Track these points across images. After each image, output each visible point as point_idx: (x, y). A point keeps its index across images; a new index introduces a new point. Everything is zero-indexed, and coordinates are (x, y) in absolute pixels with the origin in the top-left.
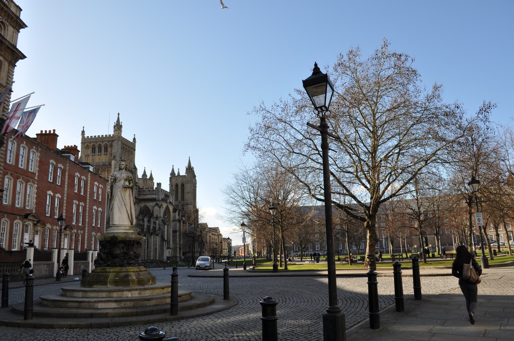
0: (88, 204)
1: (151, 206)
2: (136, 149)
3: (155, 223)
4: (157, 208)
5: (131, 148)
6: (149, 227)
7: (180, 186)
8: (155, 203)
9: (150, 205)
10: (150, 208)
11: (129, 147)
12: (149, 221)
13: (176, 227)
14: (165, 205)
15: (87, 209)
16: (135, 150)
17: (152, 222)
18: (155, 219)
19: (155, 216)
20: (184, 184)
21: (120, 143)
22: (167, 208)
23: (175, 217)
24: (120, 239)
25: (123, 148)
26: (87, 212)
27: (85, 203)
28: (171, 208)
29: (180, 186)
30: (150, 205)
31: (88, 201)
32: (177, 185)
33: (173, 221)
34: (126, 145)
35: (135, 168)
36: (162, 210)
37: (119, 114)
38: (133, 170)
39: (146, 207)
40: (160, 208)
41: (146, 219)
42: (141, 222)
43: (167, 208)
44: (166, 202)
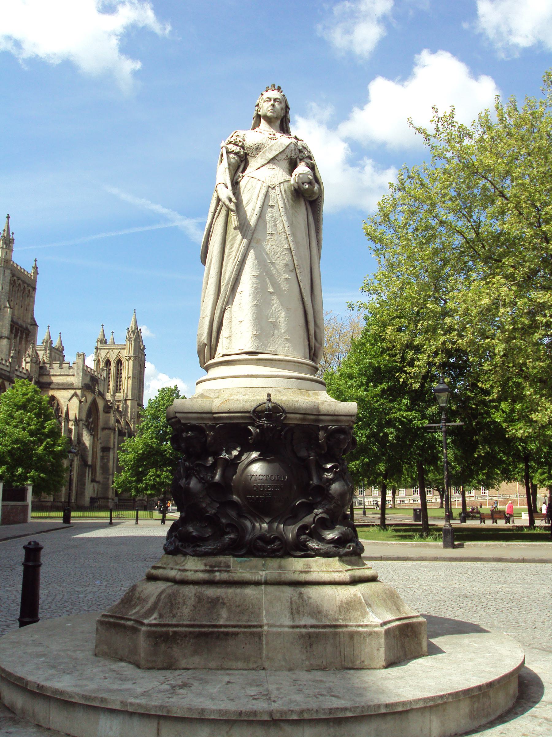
2: (38, 287)
5: (28, 285)
7: (113, 364)
8: (71, 392)
11: (24, 282)
13: (109, 441)
16: (34, 289)
20: (123, 360)
21: (8, 272)
22: (94, 403)
23: (107, 422)
24: (294, 420)
25: (13, 283)
29: (113, 364)
32: (108, 363)
33: (104, 429)
34: (19, 279)
35: (35, 325)
37: (8, 217)
38: (29, 326)
44: (93, 392)
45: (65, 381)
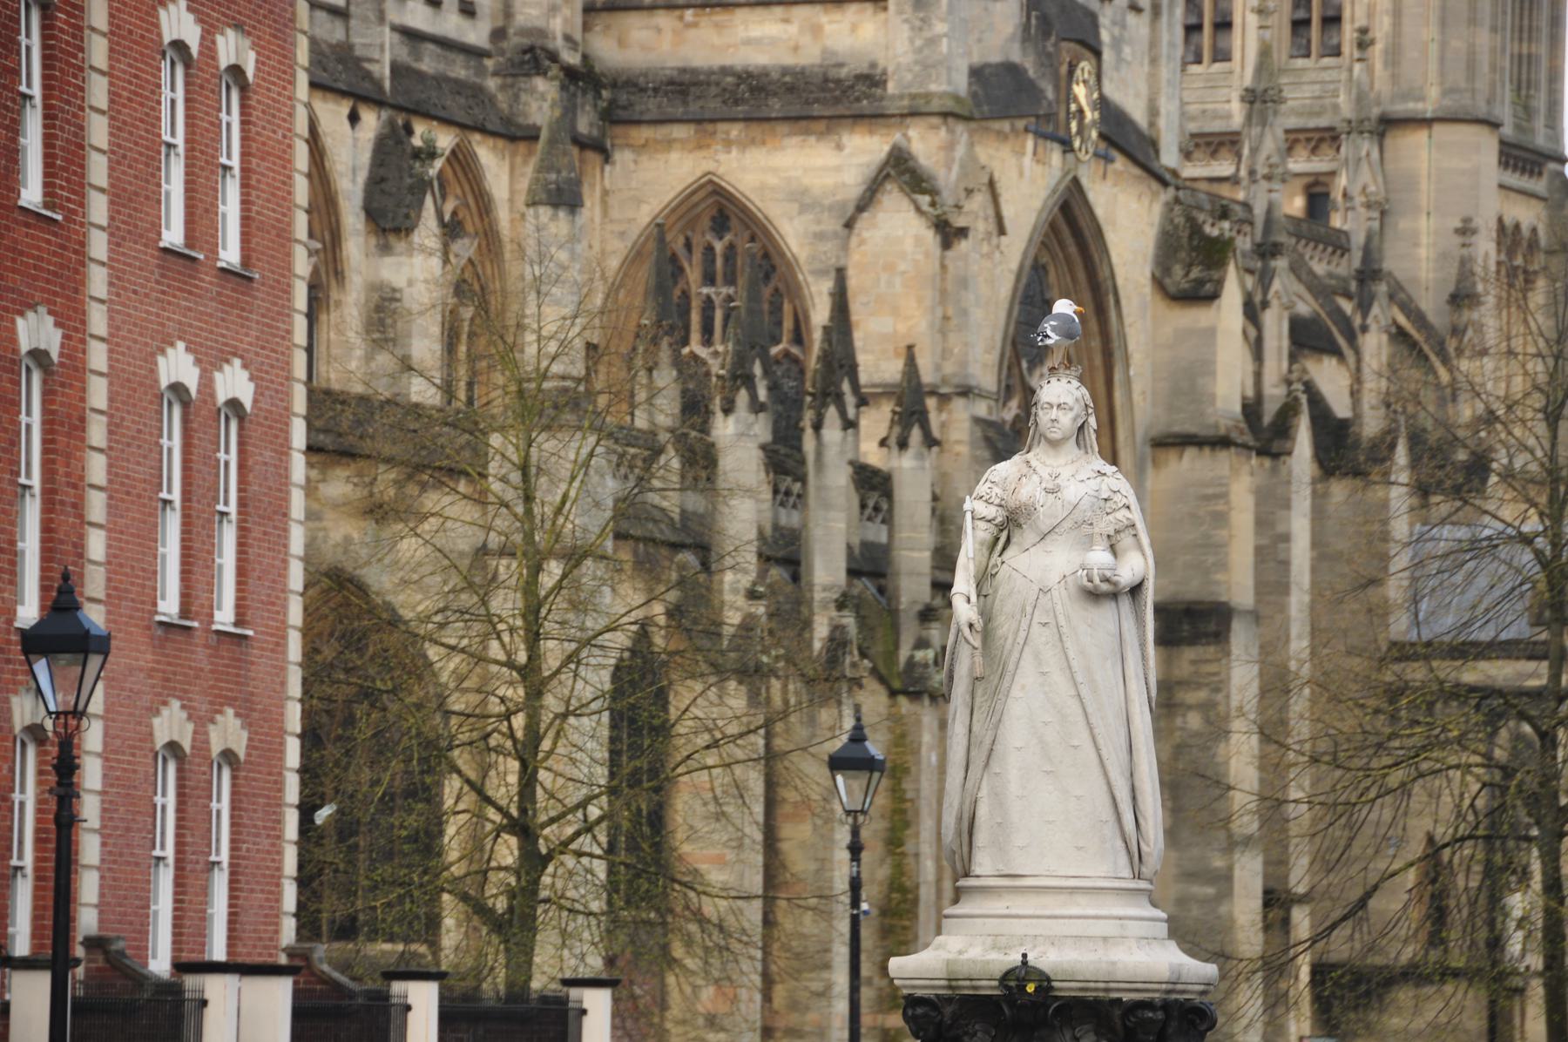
0: (98, 321)
1: (803, 201)
3: (873, 486)
4: (899, 226)
6: (784, 553)
8: (864, 150)
9: (792, 178)
10: (795, 235)
12: (785, 463)
14: (1026, 179)
15: (98, 394)
17: (839, 478)
18: (876, 421)
19: (877, 364)
22: (1071, 231)
26: (97, 432)
27: (72, 321)
28: (1130, 221)
30: (792, 178)
31: (98, 281)
36: (995, 268)
39: (719, 208)
40: (948, 233)
41: (739, 437)
42: (669, 495)
43: (1071, 231)
45: (809, 56)
